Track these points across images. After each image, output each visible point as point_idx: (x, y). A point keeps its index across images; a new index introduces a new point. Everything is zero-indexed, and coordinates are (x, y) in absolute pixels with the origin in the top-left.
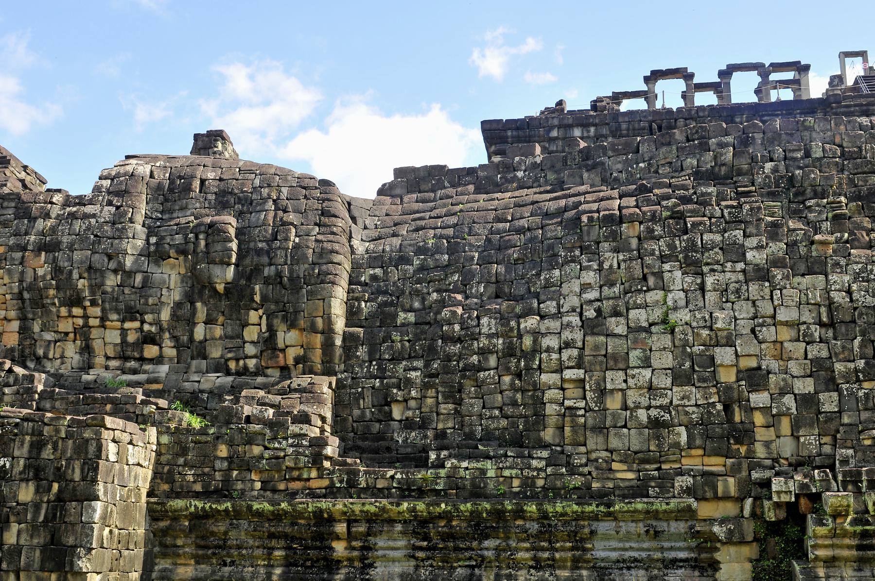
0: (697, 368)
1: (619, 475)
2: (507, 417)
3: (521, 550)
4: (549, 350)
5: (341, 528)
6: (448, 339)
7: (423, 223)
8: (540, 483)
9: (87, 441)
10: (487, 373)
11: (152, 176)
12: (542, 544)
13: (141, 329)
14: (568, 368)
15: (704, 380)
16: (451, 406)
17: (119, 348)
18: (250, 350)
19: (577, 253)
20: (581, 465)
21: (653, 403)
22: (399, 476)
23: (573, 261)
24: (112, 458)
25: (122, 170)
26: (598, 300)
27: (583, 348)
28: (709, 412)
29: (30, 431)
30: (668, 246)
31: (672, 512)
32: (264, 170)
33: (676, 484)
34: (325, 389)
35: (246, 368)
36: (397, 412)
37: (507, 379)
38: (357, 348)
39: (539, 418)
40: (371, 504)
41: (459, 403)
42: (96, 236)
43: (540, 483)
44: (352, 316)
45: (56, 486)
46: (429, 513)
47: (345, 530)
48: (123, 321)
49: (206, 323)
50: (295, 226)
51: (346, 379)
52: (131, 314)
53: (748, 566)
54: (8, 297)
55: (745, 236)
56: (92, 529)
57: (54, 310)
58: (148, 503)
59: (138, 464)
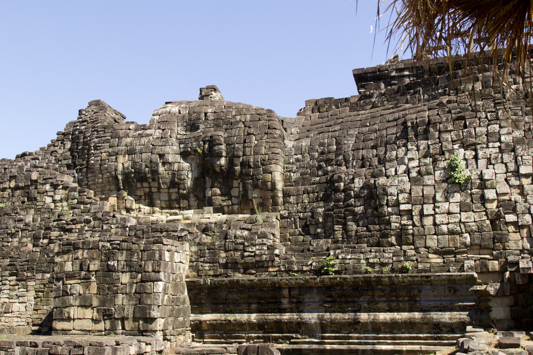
0: (474, 202)
1: (433, 261)
3: (381, 301)
5: (286, 292)
7: (322, 130)
11: (180, 113)
12: (392, 298)
13: (178, 193)
14: (402, 204)
15: (479, 208)
17: (168, 203)
20: (412, 256)
21: (450, 221)
24: (167, 259)
25: (164, 110)
26: (417, 167)
27: (410, 193)
28: (482, 225)
29: (126, 248)
30: (456, 135)
31: (463, 280)
32: (237, 106)
33: (465, 265)
34: (274, 220)
37: (370, 211)
42: (153, 145)
44: (287, 180)
46: (331, 283)
47: (287, 293)
50: (255, 135)
51: (285, 214)
53: (508, 309)
55: (501, 127)
56: (159, 295)
58: (186, 282)
59: (181, 262)
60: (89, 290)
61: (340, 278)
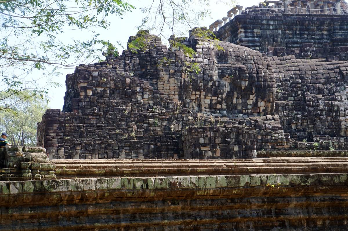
2: (330, 129)
4: (342, 110)
6: (309, 106)
8: (343, 146)
9: (251, 134)
10: (323, 116)
13: (217, 100)
16: (312, 125)
18: (249, 107)
19: (343, 83)
22: (308, 144)
23: (342, 85)
35: (248, 112)
36: (293, 127)
38: (279, 107)
39: (340, 129)
40: (303, 152)
41: (315, 125)
43: (343, 146)
45: (244, 146)
48: (212, 97)
49: (237, 98)
52: (215, 94)
54: (176, 87)
57: (190, 92)
60: (216, 154)
61: (322, 152)
